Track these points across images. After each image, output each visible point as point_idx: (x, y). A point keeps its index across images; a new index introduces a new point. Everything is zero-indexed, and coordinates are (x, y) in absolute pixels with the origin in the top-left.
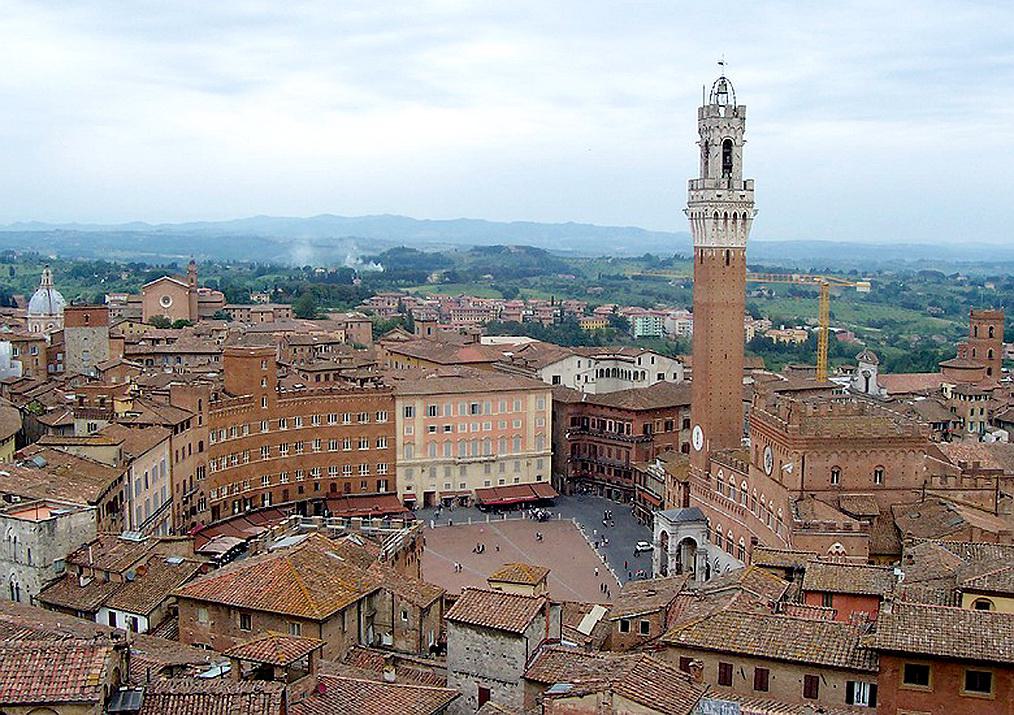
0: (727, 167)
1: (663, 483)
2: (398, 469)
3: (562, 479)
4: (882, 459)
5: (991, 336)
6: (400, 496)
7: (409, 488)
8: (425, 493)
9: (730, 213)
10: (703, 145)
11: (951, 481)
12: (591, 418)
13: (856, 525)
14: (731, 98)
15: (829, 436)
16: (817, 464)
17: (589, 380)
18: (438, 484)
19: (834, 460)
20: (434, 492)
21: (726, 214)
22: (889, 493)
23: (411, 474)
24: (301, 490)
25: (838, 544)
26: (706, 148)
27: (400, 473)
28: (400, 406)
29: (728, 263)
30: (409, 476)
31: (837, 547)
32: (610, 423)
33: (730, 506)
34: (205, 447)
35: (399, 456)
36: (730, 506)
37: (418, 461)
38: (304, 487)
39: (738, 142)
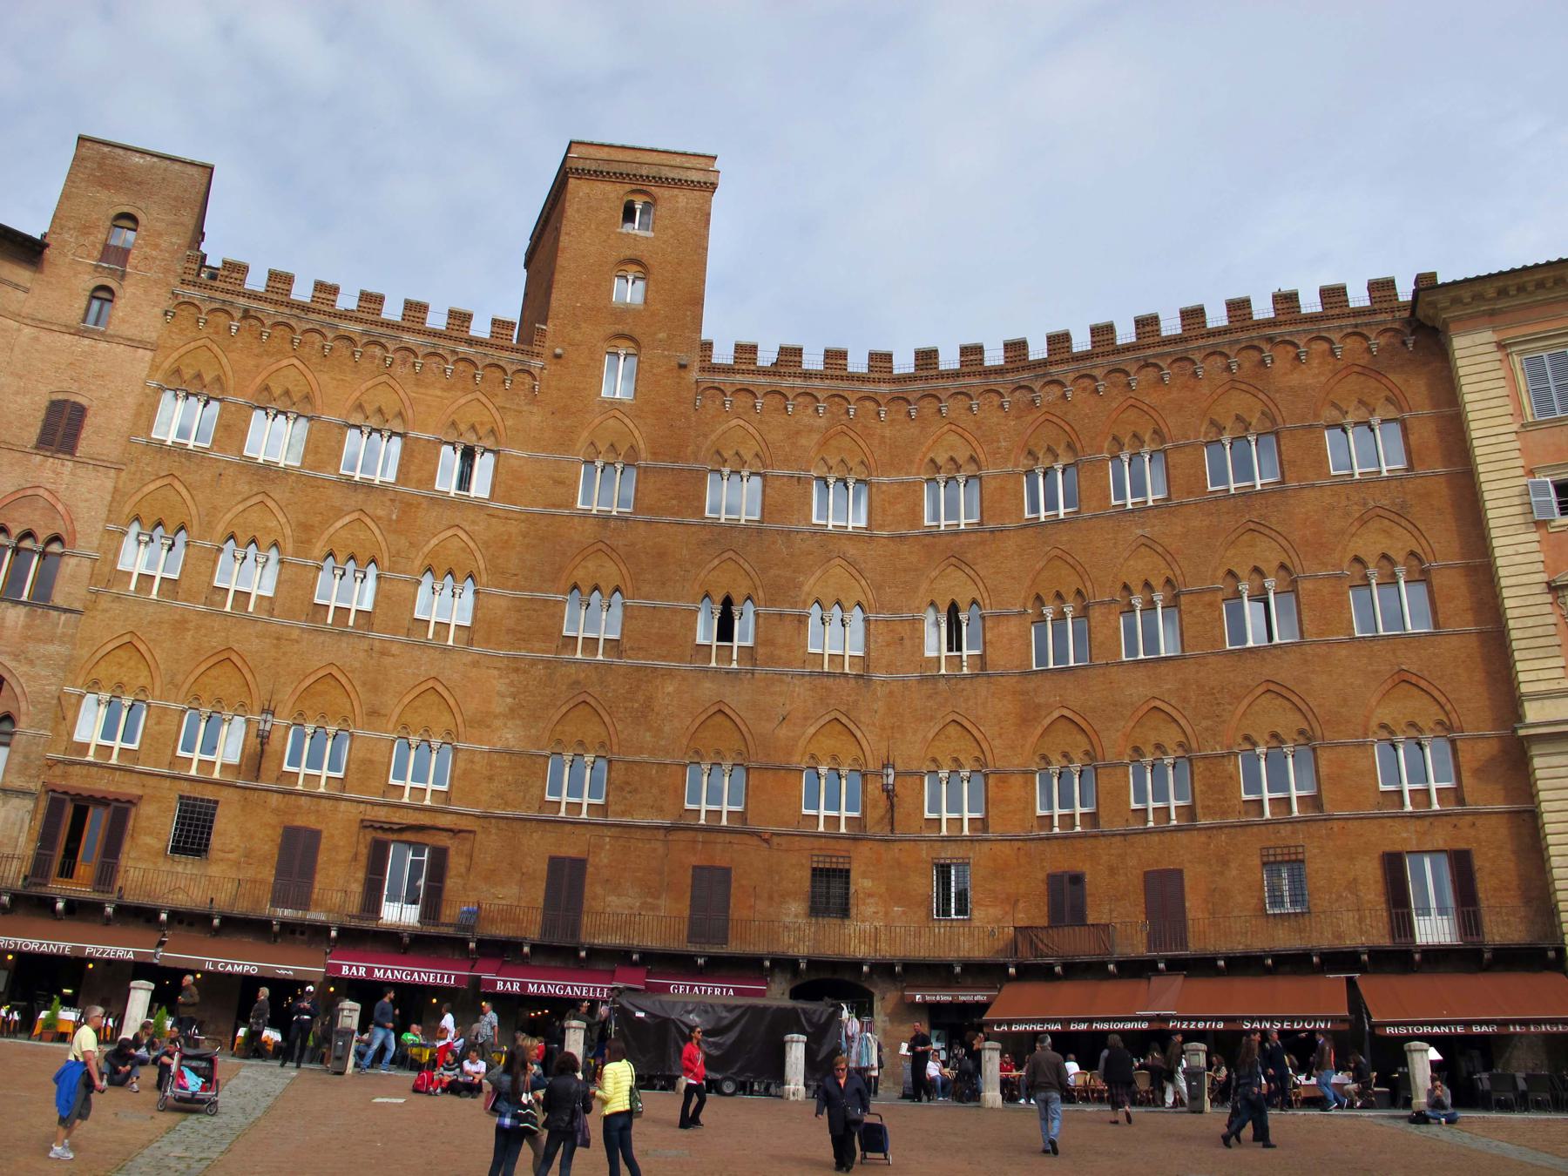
24: (830, 891)
28: (1473, 352)
38: (860, 883)
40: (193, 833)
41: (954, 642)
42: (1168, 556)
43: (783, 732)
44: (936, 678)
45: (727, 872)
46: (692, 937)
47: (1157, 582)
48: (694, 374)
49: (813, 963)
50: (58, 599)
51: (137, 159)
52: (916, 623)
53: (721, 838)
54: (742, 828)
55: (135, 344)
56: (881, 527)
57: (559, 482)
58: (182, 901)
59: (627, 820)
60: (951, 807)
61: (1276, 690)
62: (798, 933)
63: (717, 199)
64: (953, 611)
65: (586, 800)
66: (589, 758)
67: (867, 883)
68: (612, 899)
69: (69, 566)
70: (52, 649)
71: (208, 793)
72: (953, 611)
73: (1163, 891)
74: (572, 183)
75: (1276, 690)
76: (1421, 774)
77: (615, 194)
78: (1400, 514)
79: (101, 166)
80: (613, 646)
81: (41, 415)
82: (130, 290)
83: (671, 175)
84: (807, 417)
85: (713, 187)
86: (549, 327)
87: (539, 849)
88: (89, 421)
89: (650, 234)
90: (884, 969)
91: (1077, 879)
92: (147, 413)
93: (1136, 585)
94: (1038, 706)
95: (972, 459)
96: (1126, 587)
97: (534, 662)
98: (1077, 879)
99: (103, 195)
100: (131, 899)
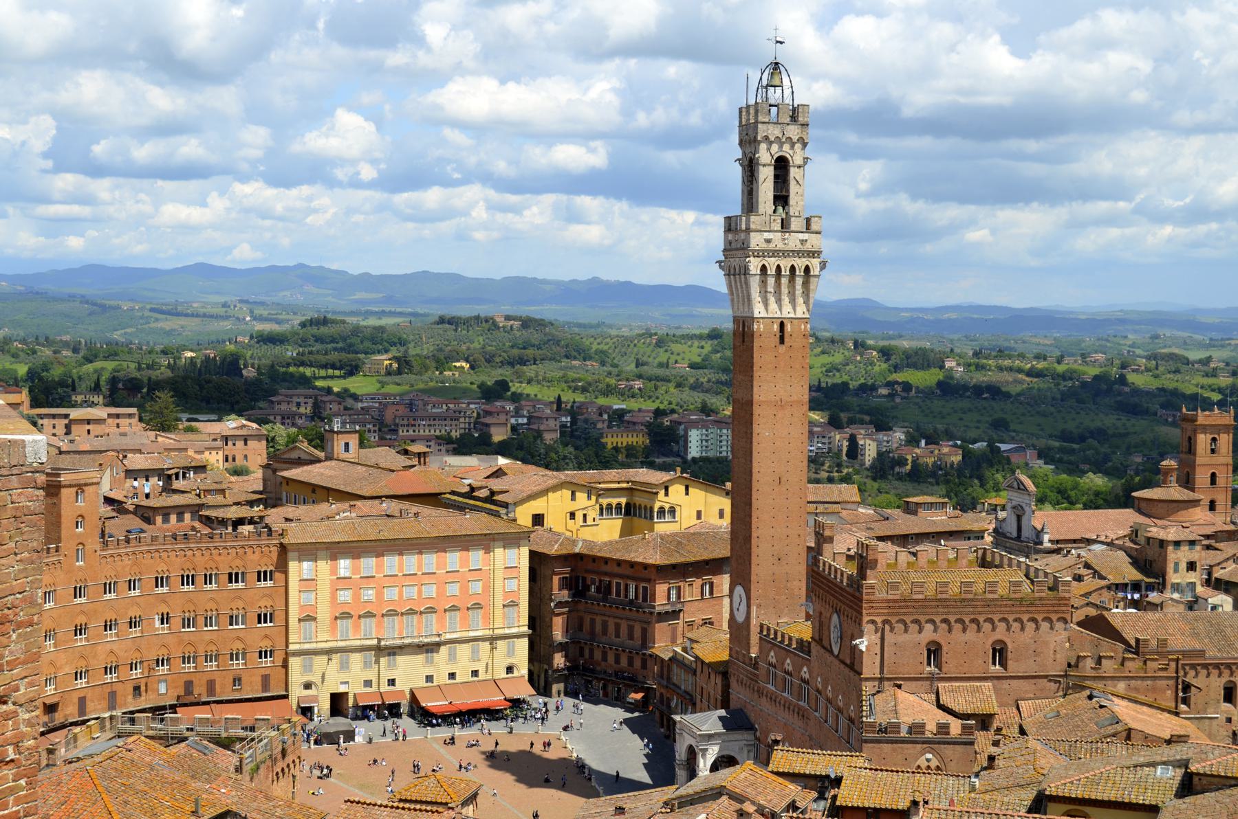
0: (781, 199)
1: (694, 673)
3: (546, 671)
4: (1000, 633)
5: (1213, 451)
7: (308, 686)
8: (332, 695)
9: (785, 264)
10: (746, 163)
11: (1108, 667)
12: (589, 577)
13: (955, 727)
14: (787, 92)
15: (921, 597)
16: (903, 638)
17: (589, 522)
18: (353, 678)
19: (928, 633)
21: (778, 267)
22: (1014, 683)
23: (311, 666)
25: (929, 756)
26: (750, 167)
29: (782, 341)
30: (308, 668)
31: (928, 760)
32: (618, 585)
33: (787, 706)
36: (787, 706)
39: (798, 160)
42: (217, 603)
61: (239, 638)
73: (211, 686)
75: (239, 638)
77: (73, 490)
78: (270, 596)
84: (126, 561)
91: (191, 682)
98: (191, 682)
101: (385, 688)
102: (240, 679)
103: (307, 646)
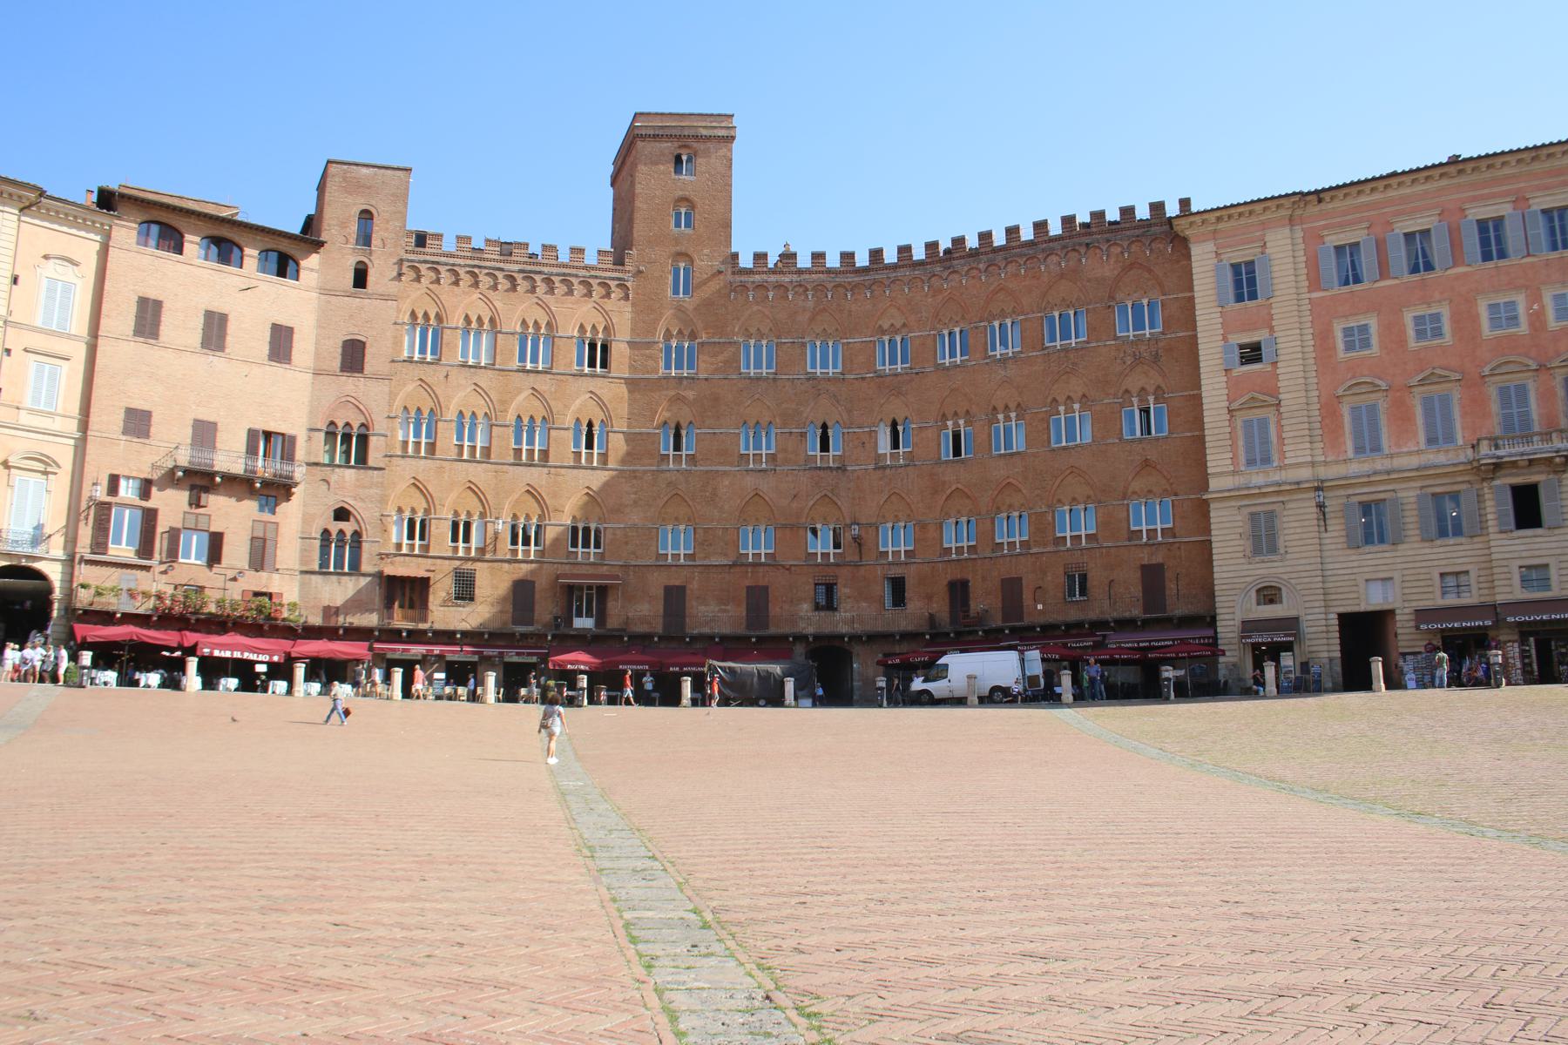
2: (1217, 515)
6: (1228, 628)
8: (1341, 616)
20: (1391, 613)
27: (1228, 532)
28: (1203, 257)
34: (374, 360)
35: (1218, 460)
37: (1305, 474)
38: (842, 591)
40: (465, 590)
41: (895, 445)
43: (794, 505)
44: (884, 468)
45: (766, 588)
46: (749, 627)
47: (1012, 405)
48: (730, 277)
49: (817, 637)
50: (371, 463)
51: (365, 171)
52: (873, 434)
53: (761, 569)
54: (773, 562)
55: (385, 298)
56: (850, 372)
57: (650, 357)
58: (465, 626)
59: (706, 562)
60: (895, 542)
62: (808, 620)
63: (735, 145)
64: (894, 425)
65: (682, 552)
66: (682, 527)
67: (847, 591)
68: (702, 608)
69: (373, 442)
70: (373, 491)
71: (469, 565)
72: (894, 425)
74: (640, 144)
76: (1152, 518)
77: (668, 147)
79: (345, 179)
80: (692, 459)
81: (340, 350)
82: (376, 262)
83: (704, 132)
85: (733, 138)
86: (634, 252)
87: (657, 583)
88: (368, 351)
89: (692, 178)
90: (855, 638)
92: (397, 343)
93: (1000, 407)
94: (944, 483)
95: (904, 325)
96: (995, 408)
97: (645, 472)
99: (350, 200)
100: (437, 626)
101: (1510, 590)
102: (1084, 578)
103: (1258, 479)
